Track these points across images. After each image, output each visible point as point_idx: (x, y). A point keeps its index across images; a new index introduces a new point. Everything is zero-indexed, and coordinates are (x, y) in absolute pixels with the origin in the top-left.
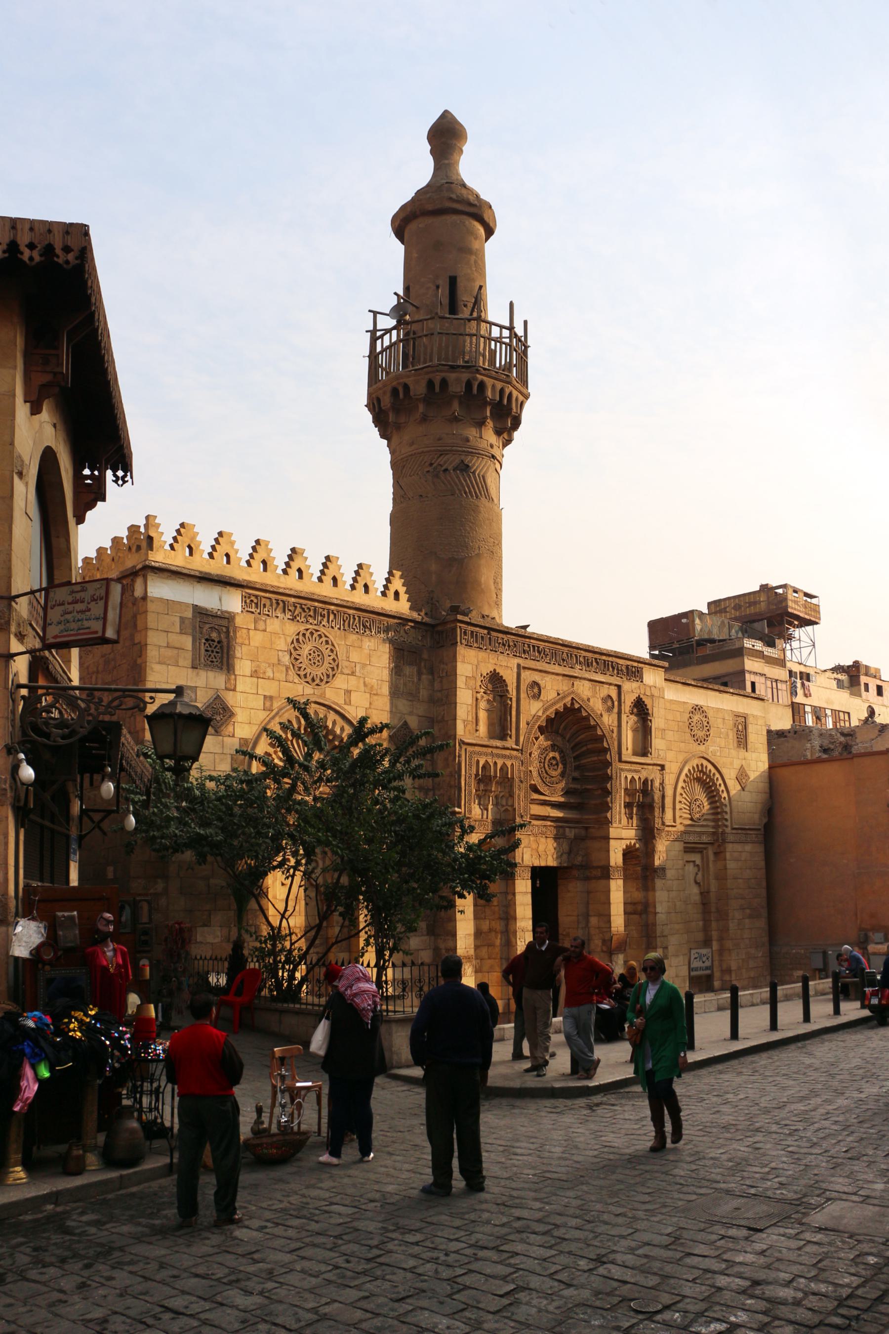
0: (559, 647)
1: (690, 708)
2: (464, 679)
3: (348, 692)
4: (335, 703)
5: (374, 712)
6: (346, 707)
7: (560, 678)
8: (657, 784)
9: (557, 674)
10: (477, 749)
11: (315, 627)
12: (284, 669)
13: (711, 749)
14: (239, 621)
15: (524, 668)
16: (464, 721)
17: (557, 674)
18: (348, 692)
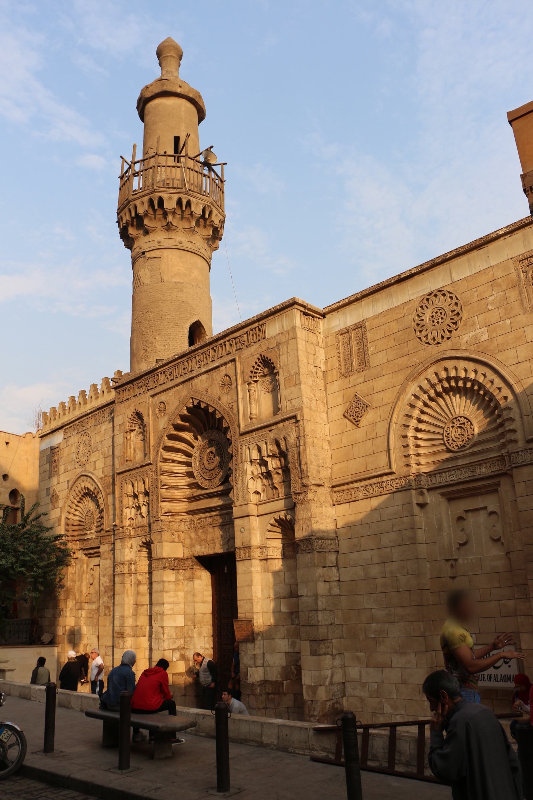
0: (179, 361)
1: (417, 304)
2: (118, 427)
3: (95, 462)
4: (90, 472)
5: (106, 468)
6: (94, 472)
7: (181, 386)
8: (292, 439)
9: (177, 385)
10: (126, 474)
11: (85, 432)
12: (73, 462)
13: (466, 338)
14: (61, 447)
15: (153, 396)
16: (118, 457)
17: (177, 385)
18: (95, 462)
